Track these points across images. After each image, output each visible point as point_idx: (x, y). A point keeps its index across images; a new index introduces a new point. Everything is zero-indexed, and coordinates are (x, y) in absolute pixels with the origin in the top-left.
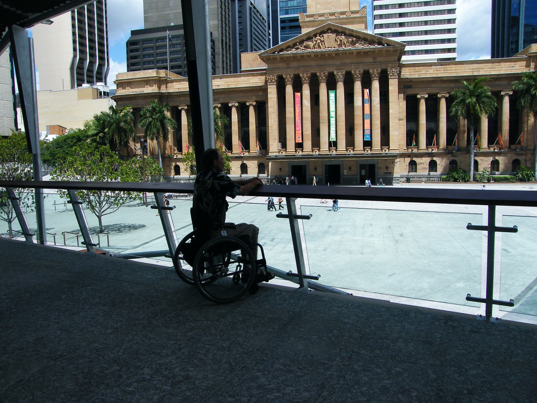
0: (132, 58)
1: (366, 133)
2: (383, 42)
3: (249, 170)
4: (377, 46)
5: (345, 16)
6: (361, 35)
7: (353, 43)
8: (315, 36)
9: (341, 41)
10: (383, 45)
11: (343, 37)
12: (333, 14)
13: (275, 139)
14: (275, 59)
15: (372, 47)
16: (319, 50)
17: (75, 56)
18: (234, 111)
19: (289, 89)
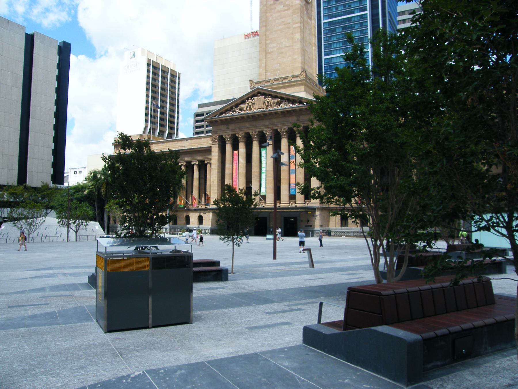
0: (197, 127)
1: (291, 187)
2: (303, 101)
3: (204, 221)
4: (297, 105)
5: (287, 81)
6: (284, 96)
7: (278, 104)
8: (248, 99)
9: (268, 102)
10: (303, 104)
11: (270, 99)
12: (277, 80)
13: (215, 193)
14: (216, 121)
15: (294, 106)
16: (250, 112)
17: (146, 127)
18: (196, 168)
19: (229, 147)
